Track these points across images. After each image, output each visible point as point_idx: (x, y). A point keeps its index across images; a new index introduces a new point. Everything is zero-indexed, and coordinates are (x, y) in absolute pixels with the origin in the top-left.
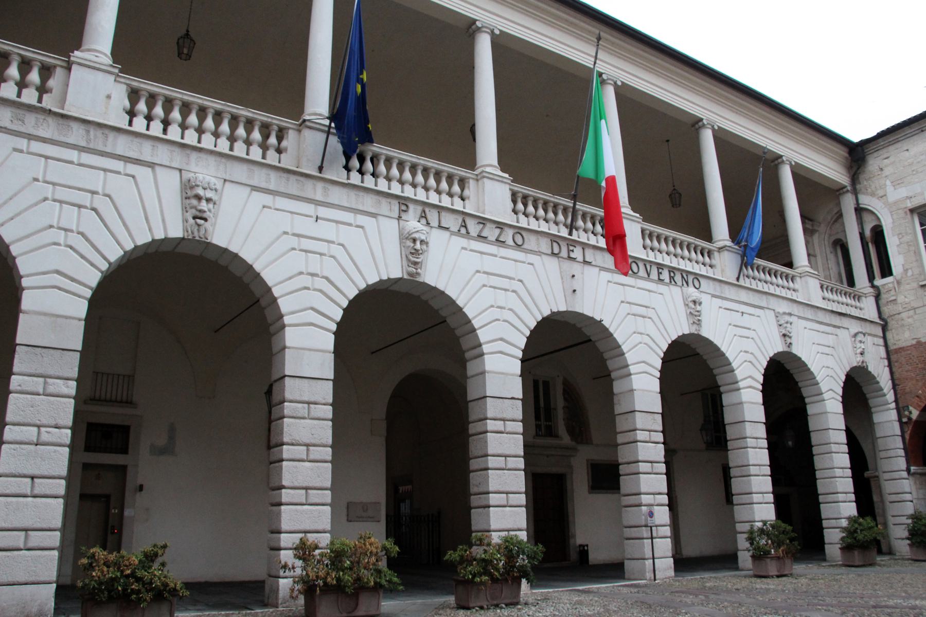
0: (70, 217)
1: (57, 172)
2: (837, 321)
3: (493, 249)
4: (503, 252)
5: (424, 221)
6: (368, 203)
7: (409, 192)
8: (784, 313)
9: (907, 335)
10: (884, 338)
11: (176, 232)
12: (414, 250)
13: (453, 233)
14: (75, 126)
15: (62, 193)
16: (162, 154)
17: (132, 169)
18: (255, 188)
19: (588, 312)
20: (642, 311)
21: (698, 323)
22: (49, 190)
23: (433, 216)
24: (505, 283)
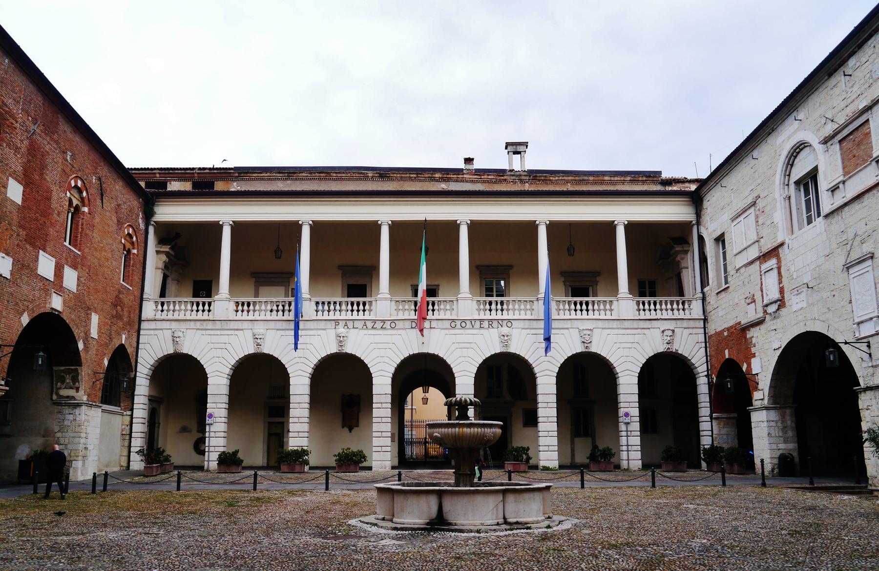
0: (219, 353)
2: (647, 324)
3: (380, 332)
4: (385, 332)
6: (322, 325)
7: (337, 316)
10: (705, 328)
15: (217, 346)
16: (245, 325)
17: (236, 332)
22: (212, 346)
23: (350, 324)
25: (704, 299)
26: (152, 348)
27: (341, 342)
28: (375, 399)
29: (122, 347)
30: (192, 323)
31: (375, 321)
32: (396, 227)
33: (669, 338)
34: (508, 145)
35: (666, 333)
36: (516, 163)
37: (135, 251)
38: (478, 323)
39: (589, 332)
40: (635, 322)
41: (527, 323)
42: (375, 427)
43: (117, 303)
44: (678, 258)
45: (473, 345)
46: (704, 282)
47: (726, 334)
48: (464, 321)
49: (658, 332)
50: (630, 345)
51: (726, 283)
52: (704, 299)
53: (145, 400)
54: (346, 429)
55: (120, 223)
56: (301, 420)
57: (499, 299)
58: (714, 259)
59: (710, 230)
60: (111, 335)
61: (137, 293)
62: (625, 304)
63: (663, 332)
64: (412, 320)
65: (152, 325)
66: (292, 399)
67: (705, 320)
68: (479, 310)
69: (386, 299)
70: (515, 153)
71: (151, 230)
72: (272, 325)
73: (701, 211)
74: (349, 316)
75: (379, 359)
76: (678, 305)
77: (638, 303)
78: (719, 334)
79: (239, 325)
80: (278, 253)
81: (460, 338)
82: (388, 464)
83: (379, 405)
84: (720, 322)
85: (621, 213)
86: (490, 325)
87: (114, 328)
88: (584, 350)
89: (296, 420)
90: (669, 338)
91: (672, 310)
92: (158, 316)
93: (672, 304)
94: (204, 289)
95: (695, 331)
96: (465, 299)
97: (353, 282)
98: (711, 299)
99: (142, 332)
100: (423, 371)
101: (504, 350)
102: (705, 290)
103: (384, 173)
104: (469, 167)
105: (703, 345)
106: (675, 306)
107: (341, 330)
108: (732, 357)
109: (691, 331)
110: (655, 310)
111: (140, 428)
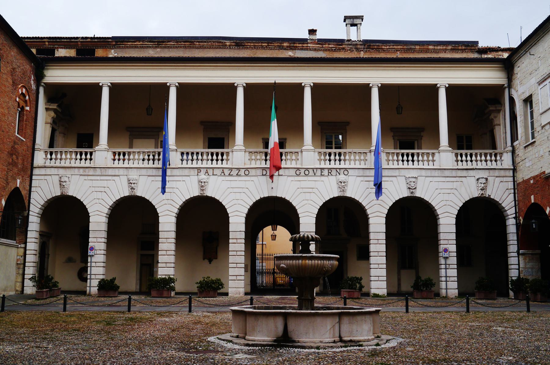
0: (99, 195)
1: (95, 183)
2: (464, 173)
5: (207, 174)
6: (186, 172)
7: (199, 165)
8: (409, 177)
10: (514, 177)
11: (127, 194)
12: (202, 185)
13: (219, 176)
14: (98, 169)
15: (97, 189)
16: (121, 172)
17: (114, 178)
18: (149, 176)
19: (279, 195)
20: (310, 190)
23: (210, 172)
24: (240, 190)
25: (513, 152)
26: (43, 190)
27: (202, 185)
28: (231, 235)
29: (17, 190)
30: (76, 169)
31: (231, 169)
32: (250, 88)
33: (483, 185)
34: (346, 18)
35: (480, 181)
36: (353, 35)
37: (28, 108)
38: (319, 171)
39: (414, 180)
40: (454, 171)
41: (361, 172)
42: (231, 259)
43: (13, 152)
44: (492, 116)
45: (314, 190)
46: (514, 137)
47: (532, 182)
48: (307, 169)
50: (449, 191)
51: (533, 137)
52: (513, 152)
53: (36, 235)
54: (206, 261)
55: (15, 84)
56: (169, 253)
57: (338, 151)
58: (523, 118)
59: (519, 93)
60: (7, 179)
61: (30, 144)
62: (445, 156)
64: (263, 169)
65: (43, 171)
66: (161, 235)
67: (514, 170)
68: (320, 160)
69: (241, 150)
70: (353, 25)
71: (41, 90)
72: (144, 172)
73: (512, 75)
74: (209, 165)
75: (235, 202)
76: (491, 157)
77: (456, 155)
78: (526, 182)
79: (116, 172)
80: (149, 111)
81: (304, 184)
82: (242, 291)
83: (235, 241)
84: (526, 173)
85: (443, 77)
86: (330, 173)
87: (11, 174)
89: (164, 253)
90: (483, 185)
91: (486, 161)
92: (48, 163)
93: (486, 156)
94: (87, 141)
95: (505, 179)
96: (308, 150)
97: (212, 136)
98: (520, 152)
99: (34, 177)
100: (272, 212)
101: (341, 194)
102: (515, 144)
103: (240, 43)
104: (313, 37)
106: (488, 158)
107: (203, 176)
108: (537, 202)
109: (502, 179)
110: (471, 161)
111: (31, 258)
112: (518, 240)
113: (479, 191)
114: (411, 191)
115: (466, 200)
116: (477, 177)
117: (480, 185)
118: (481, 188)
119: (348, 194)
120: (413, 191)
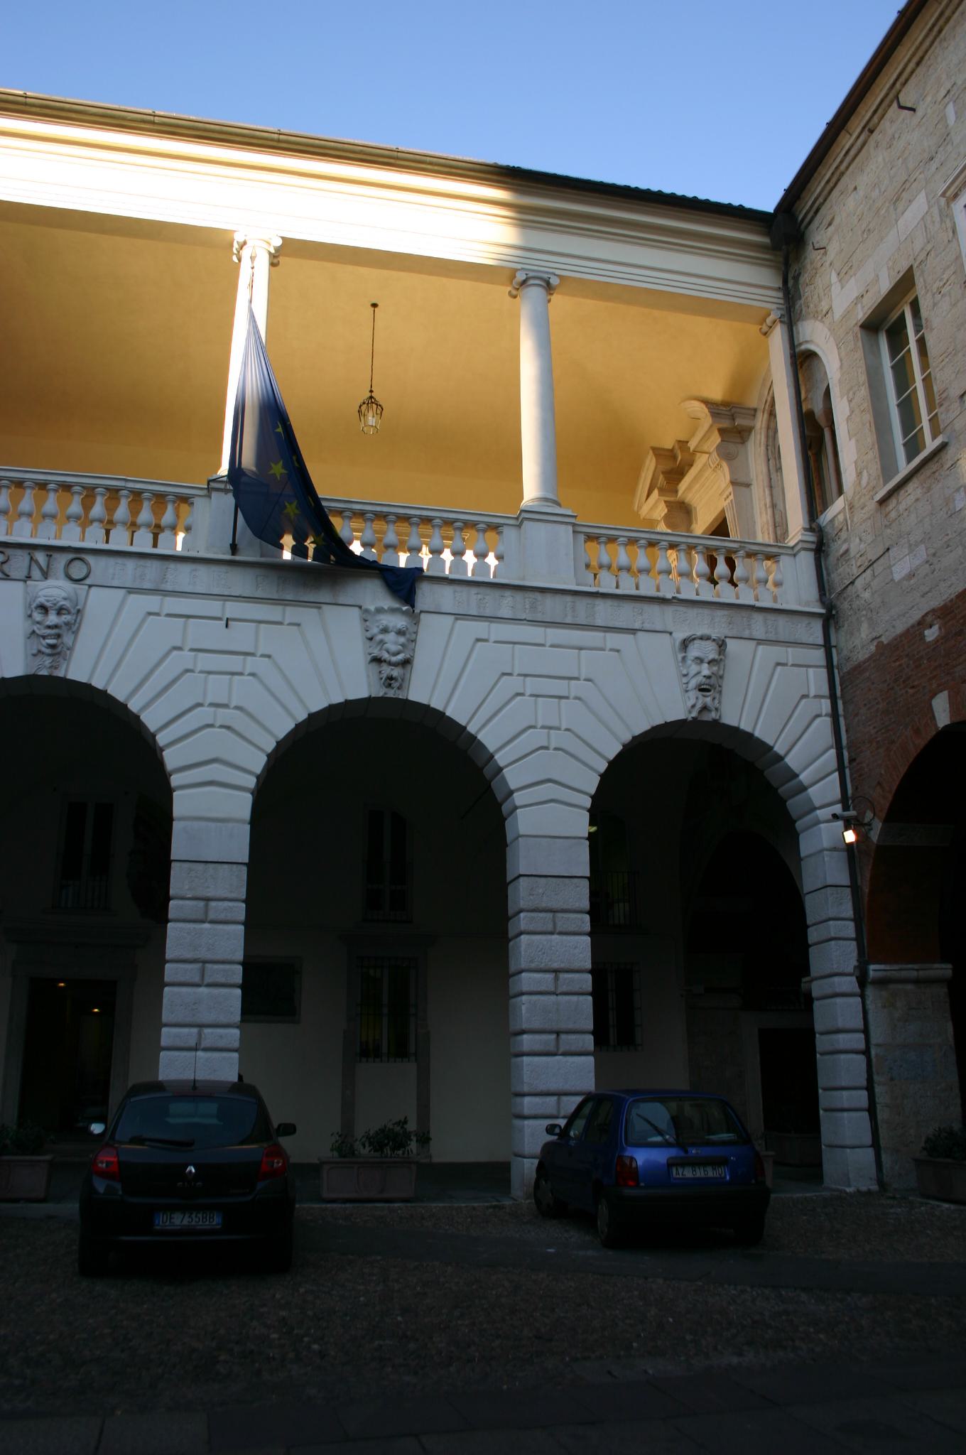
2: (625, 615)
9: (865, 632)
10: (828, 646)
21: (57, 651)
33: (706, 670)
35: (695, 650)
49: (659, 650)
50: (559, 687)
63: (685, 644)
88: (379, 692)
95: (791, 654)
105: (826, 705)
112: (857, 920)
113: (693, 694)
114: (387, 670)
115: (638, 732)
116: (680, 636)
117: (694, 668)
118: (700, 679)
119: (77, 670)
120: (396, 672)
